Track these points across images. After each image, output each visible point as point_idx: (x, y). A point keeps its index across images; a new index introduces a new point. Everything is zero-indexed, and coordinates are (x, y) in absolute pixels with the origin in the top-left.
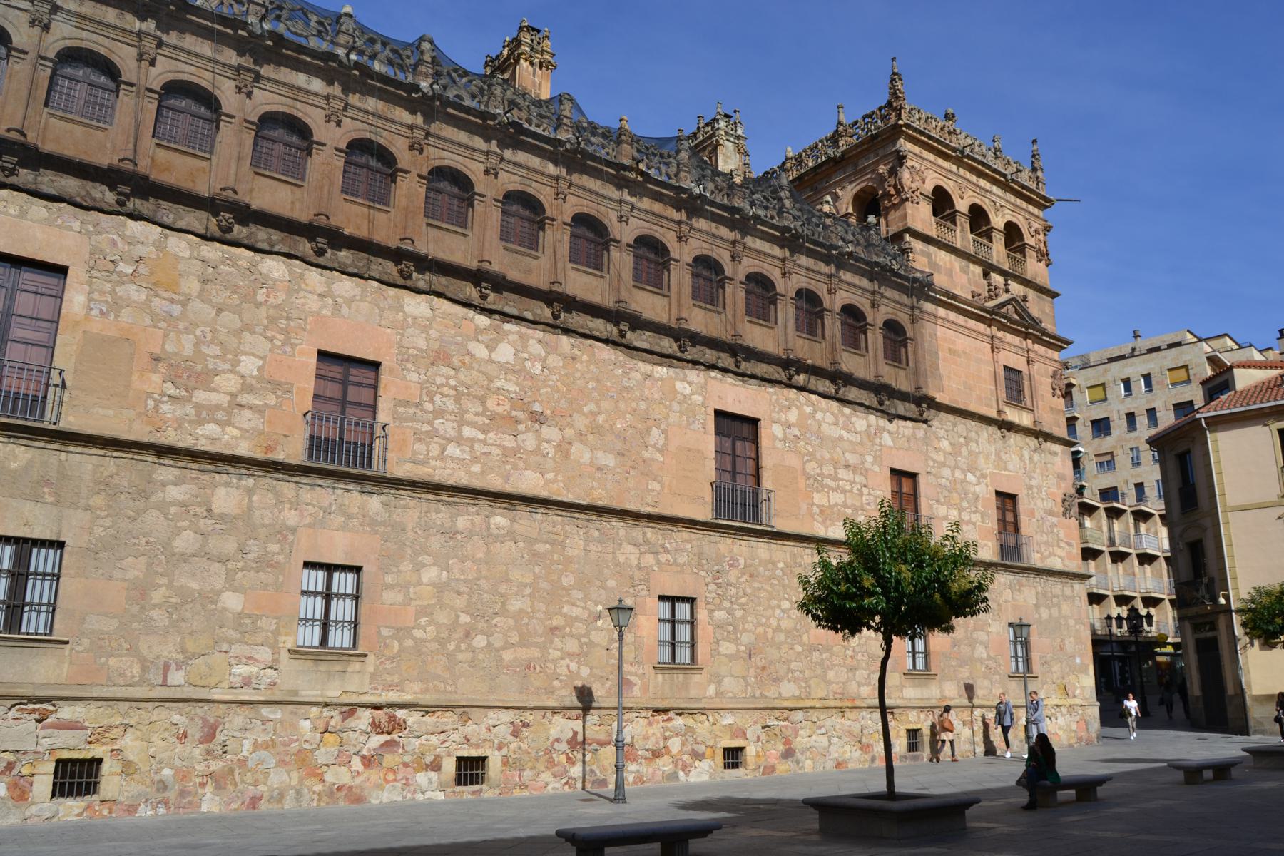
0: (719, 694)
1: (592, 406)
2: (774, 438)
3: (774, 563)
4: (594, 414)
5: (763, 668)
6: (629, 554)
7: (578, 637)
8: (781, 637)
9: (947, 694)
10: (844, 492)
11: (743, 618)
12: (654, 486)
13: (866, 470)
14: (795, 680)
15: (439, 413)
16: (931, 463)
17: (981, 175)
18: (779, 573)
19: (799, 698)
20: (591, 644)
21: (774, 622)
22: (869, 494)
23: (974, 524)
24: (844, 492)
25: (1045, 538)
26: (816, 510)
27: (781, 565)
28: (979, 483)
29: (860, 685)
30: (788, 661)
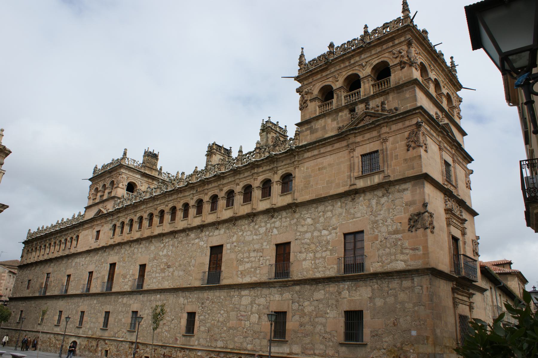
0: (199, 344)
1: (180, 259)
2: (228, 249)
3: (220, 297)
4: (180, 261)
5: (212, 336)
6: (181, 300)
7: (168, 326)
8: (220, 324)
9: (294, 351)
10: (252, 262)
11: (208, 318)
12: (191, 278)
13: (263, 249)
14: (223, 340)
15: (153, 272)
16: (298, 234)
17: (349, 58)
18: (221, 300)
19: (223, 348)
20: (171, 328)
21: (217, 319)
22: (263, 259)
23: (324, 258)
24: (252, 262)
25: (387, 250)
26: (239, 272)
27: (222, 297)
28: (330, 234)
29: (248, 344)
30: (221, 333)
